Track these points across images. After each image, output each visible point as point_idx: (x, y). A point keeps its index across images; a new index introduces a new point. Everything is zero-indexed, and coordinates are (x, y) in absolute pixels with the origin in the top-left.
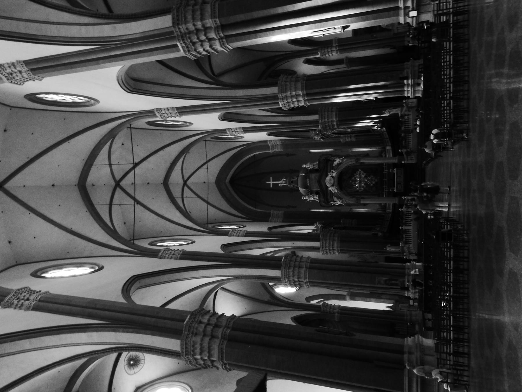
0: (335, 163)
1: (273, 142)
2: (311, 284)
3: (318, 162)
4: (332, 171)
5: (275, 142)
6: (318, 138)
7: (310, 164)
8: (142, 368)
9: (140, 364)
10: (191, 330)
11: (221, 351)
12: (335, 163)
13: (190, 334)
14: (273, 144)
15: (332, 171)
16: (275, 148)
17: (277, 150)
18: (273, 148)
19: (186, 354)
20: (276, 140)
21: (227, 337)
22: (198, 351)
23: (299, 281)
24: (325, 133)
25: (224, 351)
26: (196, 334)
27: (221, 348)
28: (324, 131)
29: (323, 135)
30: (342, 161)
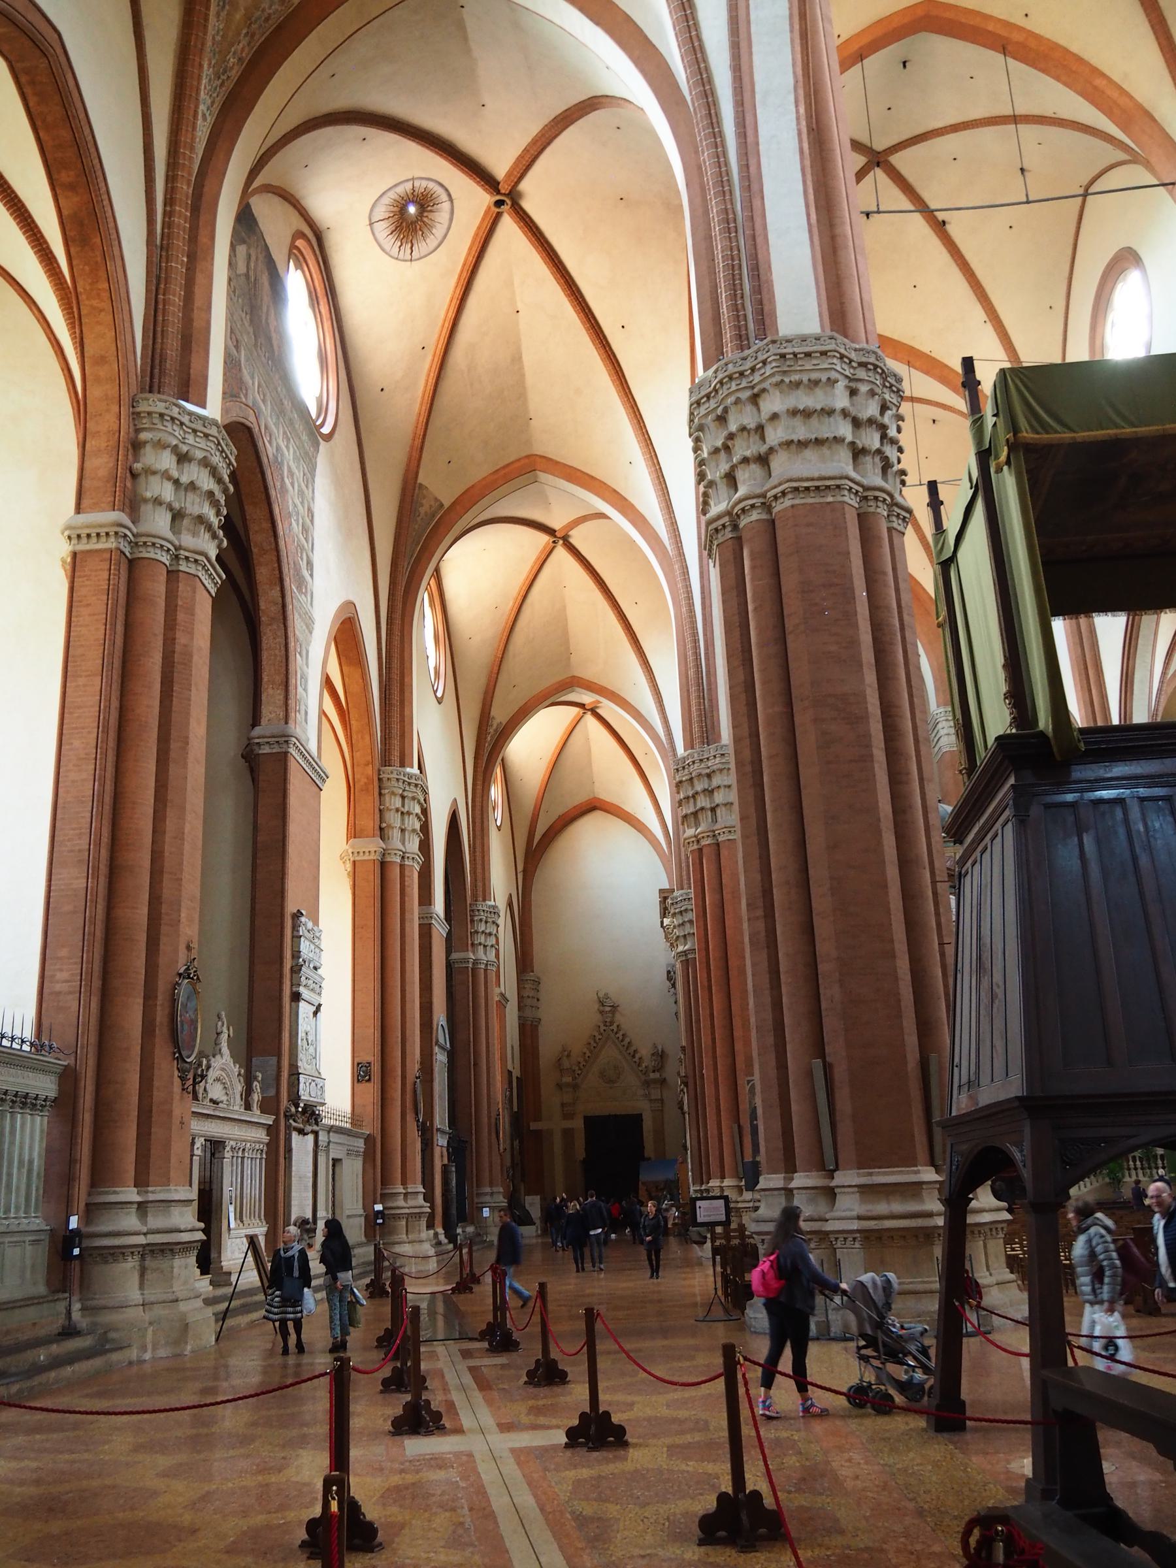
2: (705, 851)
8: (383, 250)
9: (399, 243)
10: (862, 374)
11: (828, 487)
13: (852, 371)
17: (942, 732)
19: (783, 356)
21: (872, 510)
22: (805, 400)
23: (713, 810)
25: (830, 499)
26: (853, 392)
27: (838, 487)
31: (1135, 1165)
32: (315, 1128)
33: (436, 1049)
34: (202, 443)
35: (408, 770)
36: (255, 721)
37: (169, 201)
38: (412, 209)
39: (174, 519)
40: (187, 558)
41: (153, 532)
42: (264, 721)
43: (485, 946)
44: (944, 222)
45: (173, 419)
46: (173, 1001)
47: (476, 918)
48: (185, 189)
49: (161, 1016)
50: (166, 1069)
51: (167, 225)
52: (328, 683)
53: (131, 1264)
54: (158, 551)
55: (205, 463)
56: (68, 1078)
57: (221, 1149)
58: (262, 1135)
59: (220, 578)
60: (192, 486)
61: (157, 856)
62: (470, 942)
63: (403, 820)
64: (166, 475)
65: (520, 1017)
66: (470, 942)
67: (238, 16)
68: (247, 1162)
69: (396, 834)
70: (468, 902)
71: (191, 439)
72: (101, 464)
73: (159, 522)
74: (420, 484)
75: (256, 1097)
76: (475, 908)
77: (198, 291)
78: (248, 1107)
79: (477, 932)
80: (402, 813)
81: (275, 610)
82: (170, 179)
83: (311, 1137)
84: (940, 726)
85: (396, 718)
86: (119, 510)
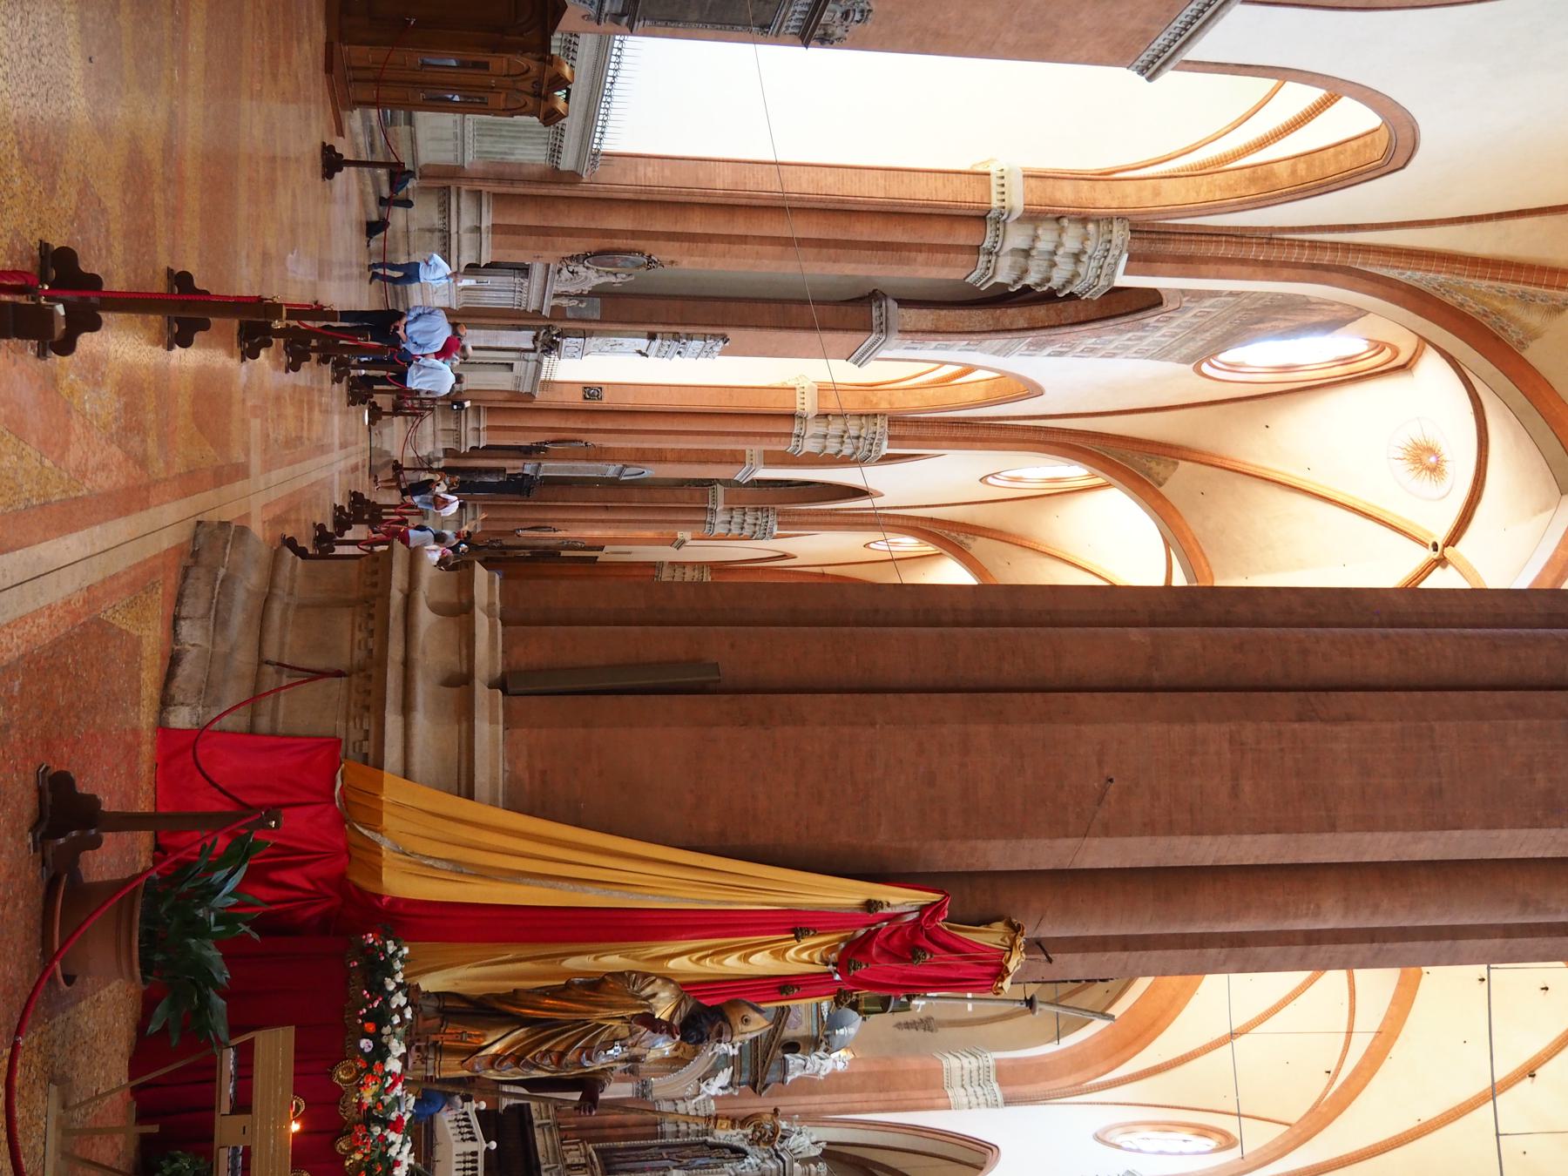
0: (724, 1077)
1: (982, 1099)
3: (789, 1079)
4: (736, 1052)
5: (973, 1099)
6: (795, 1139)
7: (818, 1073)
12: (724, 1077)
14: (978, 1089)
15: (736, 1052)
16: (975, 1074)
17: (965, 1061)
18: (981, 1072)
20: (970, 1108)
24: (771, 1158)
28: (771, 1170)
29: (778, 1156)
30: (699, 1088)
31: (468, 1169)
32: (539, 350)
33: (620, 466)
34: (1092, 273)
35: (885, 443)
36: (903, 303)
37: (1314, 245)
38: (1433, 459)
39: (1024, 250)
40: (990, 261)
41: (1008, 233)
42: (902, 311)
43: (730, 522)
44: (1533, 1076)
45: (1108, 250)
46: (630, 252)
47: (759, 513)
48: (1326, 258)
49: (618, 243)
50: (580, 246)
51: (1292, 244)
52: (969, 369)
53: (436, 220)
54: (992, 240)
55: (1076, 275)
56: (574, 177)
57: (522, 275)
58: (533, 306)
59: (982, 285)
60: (1053, 265)
61: (743, 239)
62: (735, 506)
63: (835, 437)
64: (1059, 245)
65: (662, 563)
66: (735, 506)
67: (1496, 303)
68: (511, 294)
69: (821, 430)
70: (776, 506)
71: (1094, 264)
72: (1066, 195)
73: (1016, 238)
74: (1177, 464)
75: (564, 302)
76: (771, 512)
77: (1235, 269)
78: (556, 296)
79: (744, 514)
80: (842, 437)
81: (1007, 323)
82: (1335, 246)
83: (531, 346)
84: (973, 1059)
85: (937, 432)
86: (1025, 211)
